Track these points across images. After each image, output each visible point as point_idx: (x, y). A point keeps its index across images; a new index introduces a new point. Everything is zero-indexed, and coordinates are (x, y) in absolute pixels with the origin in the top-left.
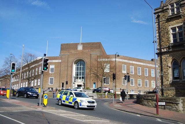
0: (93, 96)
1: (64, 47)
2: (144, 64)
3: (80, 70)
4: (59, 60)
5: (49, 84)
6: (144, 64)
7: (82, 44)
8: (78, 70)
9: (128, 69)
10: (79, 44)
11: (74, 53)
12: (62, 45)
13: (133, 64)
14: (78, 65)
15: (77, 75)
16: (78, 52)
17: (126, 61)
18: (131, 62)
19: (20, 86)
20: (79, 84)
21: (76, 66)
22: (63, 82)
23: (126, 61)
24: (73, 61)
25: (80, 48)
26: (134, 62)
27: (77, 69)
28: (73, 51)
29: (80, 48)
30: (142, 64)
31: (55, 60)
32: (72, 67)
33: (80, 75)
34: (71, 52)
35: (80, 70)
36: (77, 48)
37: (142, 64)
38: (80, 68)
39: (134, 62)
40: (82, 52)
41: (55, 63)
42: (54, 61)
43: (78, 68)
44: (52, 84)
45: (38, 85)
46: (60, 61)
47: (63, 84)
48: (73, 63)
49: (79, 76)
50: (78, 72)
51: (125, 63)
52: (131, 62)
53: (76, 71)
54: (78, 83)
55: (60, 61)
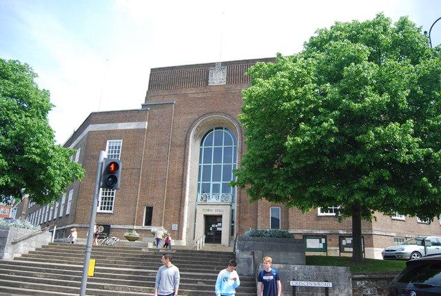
1: (162, 79)
3: (218, 160)
4: (139, 120)
7: (224, 64)
8: (207, 159)
10: (213, 65)
11: (196, 96)
12: (155, 73)
14: (209, 143)
16: (209, 95)
19: (44, 220)
21: (203, 147)
25: (218, 78)
27: (206, 156)
28: (191, 92)
29: (218, 78)
31: (125, 124)
33: (216, 178)
34: (186, 95)
35: (218, 160)
38: (218, 151)
41: (126, 131)
43: (208, 152)
44: (109, 211)
46: (145, 125)
48: (189, 132)
49: (212, 183)
50: (207, 169)
53: (202, 165)
55: (145, 125)
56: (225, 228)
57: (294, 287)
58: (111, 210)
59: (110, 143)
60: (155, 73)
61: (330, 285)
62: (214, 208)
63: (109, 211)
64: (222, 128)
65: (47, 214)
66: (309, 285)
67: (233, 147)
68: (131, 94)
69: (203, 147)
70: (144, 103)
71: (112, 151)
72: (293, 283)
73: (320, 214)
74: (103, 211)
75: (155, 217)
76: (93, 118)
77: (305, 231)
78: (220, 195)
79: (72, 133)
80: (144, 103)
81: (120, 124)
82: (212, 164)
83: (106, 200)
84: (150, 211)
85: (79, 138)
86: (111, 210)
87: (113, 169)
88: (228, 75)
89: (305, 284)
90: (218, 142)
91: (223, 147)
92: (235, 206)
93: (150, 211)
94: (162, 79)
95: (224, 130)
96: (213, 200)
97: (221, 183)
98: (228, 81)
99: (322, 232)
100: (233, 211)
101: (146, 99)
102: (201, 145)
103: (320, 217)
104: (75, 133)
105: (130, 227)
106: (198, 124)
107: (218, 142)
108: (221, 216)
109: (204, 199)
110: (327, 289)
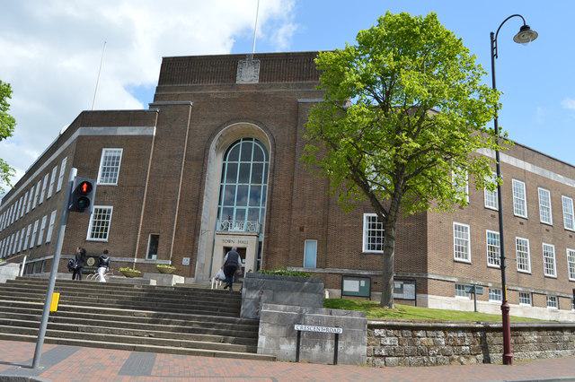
0: (337, 336)
1: (175, 70)
2: (537, 170)
5: (88, 238)
6: (537, 170)
7: (257, 56)
10: (243, 57)
14: (234, 157)
15: (230, 201)
19: (17, 248)
20: (235, 244)
21: (227, 162)
24: (213, 135)
25: (248, 76)
27: (229, 173)
28: (214, 90)
29: (248, 76)
30: (528, 167)
31: (127, 128)
32: (202, 160)
37: (528, 167)
38: (245, 169)
42: (122, 131)
43: (232, 169)
44: (103, 239)
45: (47, 241)
48: (209, 142)
49: (235, 208)
54: (230, 238)
56: (248, 264)
57: (299, 332)
58: (105, 237)
59: (106, 151)
61: (340, 331)
62: (237, 239)
63: (103, 239)
64: (251, 139)
65: (21, 241)
66: (307, 329)
67: (264, 163)
69: (227, 162)
70: (152, 102)
71: (109, 163)
72: (297, 327)
73: (364, 250)
74: (94, 239)
75: (162, 247)
76: (86, 118)
77: (346, 271)
78: (245, 224)
79: (55, 137)
80: (152, 102)
81: (120, 128)
82: (237, 184)
83: (99, 225)
84: (155, 240)
85: (67, 144)
86: (105, 237)
87: (85, 190)
89: (312, 329)
90: (246, 157)
92: (262, 238)
93: (155, 240)
94: (175, 70)
95: (253, 142)
96: (236, 229)
97: (247, 208)
98: (261, 79)
99: (366, 273)
100: (260, 243)
101: (156, 97)
102: (225, 160)
103: (365, 254)
104: (61, 136)
105: (129, 260)
106: (220, 133)
107: (246, 157)
108: (245, 249)
109: (225, 228)
110: (337, 335)
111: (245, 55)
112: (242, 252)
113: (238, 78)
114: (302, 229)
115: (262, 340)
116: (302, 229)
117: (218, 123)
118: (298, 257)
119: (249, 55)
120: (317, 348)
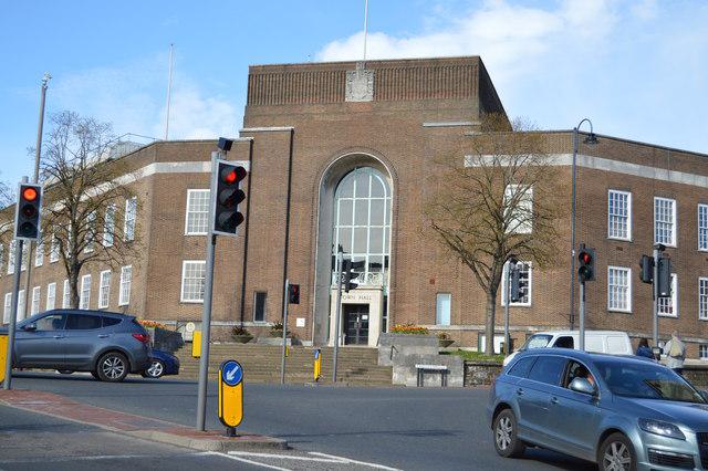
1: (269, 88)
7: (368, 65)
9: (644, 218)
10: (351, 65)
12: (252, 69)
13: (671, 190)
16: (347, 118)
17: (633, 169)
18: (661, 175)
22: (261, 288)
23: (633, 169)
25: (360, 91)
26: (678, 177)
28: (318, 112)
29: (360, 91)
36: (342, 94)
39: (678, 177)
40: (369, 114)
47: (261, 297)
51: (626, 182)
52: (661, 175)
60: (252, 69)
68: (224, 118)
70: (241, 128)
88: (376, 84)
91: (370, 199)
92: (388, 292)
94: (269, 88)
100: (385, 297)
111: (355, 62)
112: (365, 308)
113: (347, 93)
114: (432, 282)
115: (395, 376)
116: (432, 282)
117: (327, 153)
118: (432, 313)
119: (359, 62)
120: (431, 379)
